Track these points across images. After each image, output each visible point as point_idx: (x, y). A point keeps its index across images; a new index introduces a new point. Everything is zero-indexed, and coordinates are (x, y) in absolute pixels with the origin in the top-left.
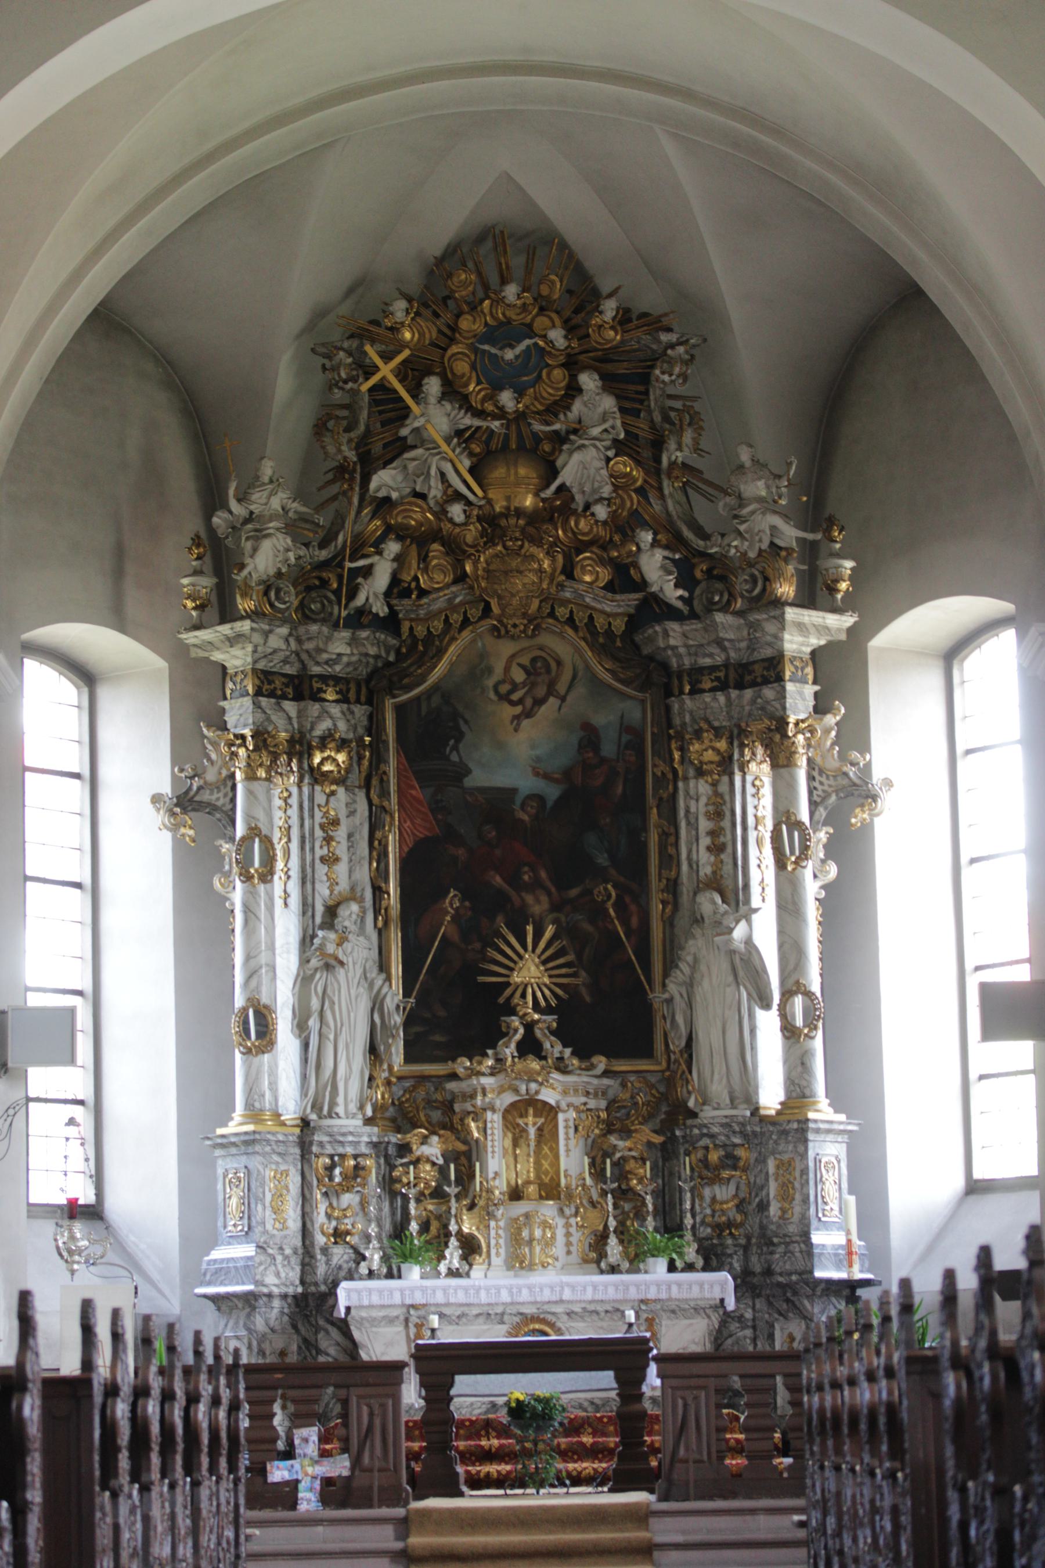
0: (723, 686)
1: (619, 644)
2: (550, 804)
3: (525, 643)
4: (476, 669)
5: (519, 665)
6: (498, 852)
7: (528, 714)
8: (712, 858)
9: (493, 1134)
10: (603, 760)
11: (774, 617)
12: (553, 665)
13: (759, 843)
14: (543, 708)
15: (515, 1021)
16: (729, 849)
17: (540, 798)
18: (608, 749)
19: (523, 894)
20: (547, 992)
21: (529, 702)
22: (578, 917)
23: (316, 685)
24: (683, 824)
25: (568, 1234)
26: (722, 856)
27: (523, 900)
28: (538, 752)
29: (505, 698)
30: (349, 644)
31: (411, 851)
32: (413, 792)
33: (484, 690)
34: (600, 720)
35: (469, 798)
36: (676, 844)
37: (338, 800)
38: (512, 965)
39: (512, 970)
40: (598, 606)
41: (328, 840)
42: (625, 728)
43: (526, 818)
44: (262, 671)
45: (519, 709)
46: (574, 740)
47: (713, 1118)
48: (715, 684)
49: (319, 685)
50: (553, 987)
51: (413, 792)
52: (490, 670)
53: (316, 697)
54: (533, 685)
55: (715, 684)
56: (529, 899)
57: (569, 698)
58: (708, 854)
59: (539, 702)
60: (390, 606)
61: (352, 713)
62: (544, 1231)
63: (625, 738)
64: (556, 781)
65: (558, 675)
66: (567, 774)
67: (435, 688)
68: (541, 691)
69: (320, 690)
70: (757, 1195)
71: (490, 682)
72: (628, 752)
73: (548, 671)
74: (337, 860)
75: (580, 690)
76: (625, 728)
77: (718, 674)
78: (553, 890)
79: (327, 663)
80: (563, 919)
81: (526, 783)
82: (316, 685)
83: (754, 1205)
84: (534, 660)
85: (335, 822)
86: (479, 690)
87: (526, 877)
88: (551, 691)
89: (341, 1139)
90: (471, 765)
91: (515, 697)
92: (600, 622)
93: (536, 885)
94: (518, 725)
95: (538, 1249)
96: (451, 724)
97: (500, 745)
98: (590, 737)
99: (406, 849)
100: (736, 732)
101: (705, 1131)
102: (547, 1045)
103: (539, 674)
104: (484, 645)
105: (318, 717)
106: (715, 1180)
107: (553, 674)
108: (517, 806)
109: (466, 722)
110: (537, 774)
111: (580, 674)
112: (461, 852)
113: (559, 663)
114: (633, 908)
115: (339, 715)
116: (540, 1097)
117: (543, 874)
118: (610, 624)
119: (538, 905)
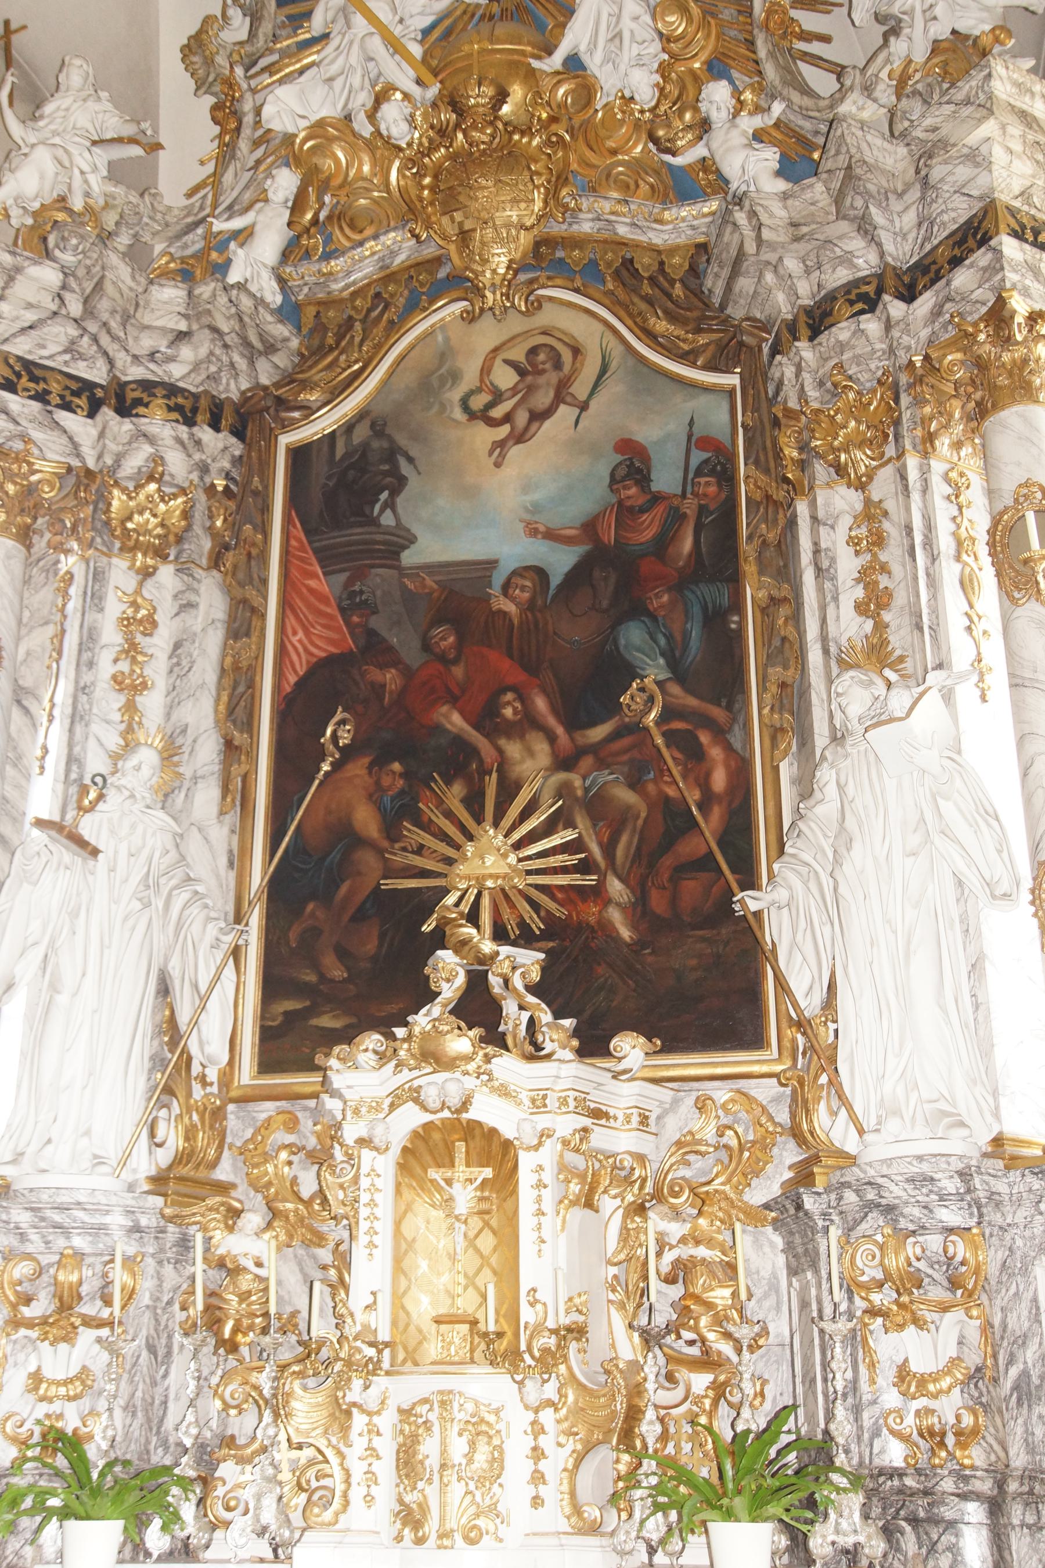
0: (871, 304)
1: (678, 290)
2: (555, 581)
3: (516, 324)
4: (434, 376)
5: (506, 362)
6: (458, 671)
7: (520, 437)
8: (869, 625)
9: (372, 1203)
10: (657, 498)
11: (967, 102)
12: (567, 356)
13: (967, 585)
14: (547, 424)
15: (446, 957)
16: (900, 598)
17: (540, 574)
18: (666, 478)
19: (502, 742)
20: (524, 907)
21: (522, 418)
22: (605, 777)
23: (131, 395)
24: (808, 577)
25: (538, 1453)
26: (887, 616)
27: (500, 751)
28: (536, 496)
29: (483, 416)
30: (186, 316)
31: (302, 683)
32: (312, 583)
33: (443, 407)
34: (647, 433)
35: (411, 586)
36: (797, 618)
37: (159, 587)
38: (451, 852)
39: (450, 861)
40: (643, 238)
41: (131, 650)
42: (697, 440)
43: (511, 608)
44: (19, 358)
45: (505, 430)
46: (604, 471)
47: (888, 1162)
48: (860, 306)
49: (137, 394)
50: (535, 894)
51: (312, 583)
52: (455, 376)
53: (124, 410)
54: (531, 389)
55: (860, 306)
56: (513, 749)
57: (593, 404)
58: (860, 619)
59: (539, 416)
60: (282, 281)
61: (198, 443)
62: (472, 1444)
63: (698, 457)
64: (568, 541)
65: (574, 371)
66: (590, 528)
67: (362, 415)
68: (543, 399)
69: (138, 402)
70: (1011, 1361)
71: (455, 395)
72: (703, 480)
73: (558, 365)
74: (144, 686)
75: (614, 388)
76: (697, 440)
77: (865, 289)
78: (560, 730)
79: (152, 356)
80: (578, 783)
81: (510, 548)
82: (131, 395)
83: (1008, 1384)
84: (533, 351)
85: (150, 624)
86: (436, 408)
87: (508, 712)
88: (560, 396)
89: (57, 1217)
90: (416, 529)
91: (497, 413)
92: (645, 263)
93: (530, 722)
94: (502, 456)
95: (457, 1490)
96: (387, 467)
97: (470, 492)
98: (633, 464)
99: (293, 679)
100: (904, 379)
101: (871, 1195)
102: (510, 1007)
103: (543, 372)
104: (447, 340)
105: (129, 443)
106: (906, 1316)
107: (567, 368)
108: (496, 590)
109: (411, 460)
110: (533, 532)
111: (614, 365)
112: (391, 678)
113: (576, 351)
114: (716, 753)
115: (170, 442)
116: (472, 1114)
117: (541, 704)
118: (662, 263)
119: (532, 763)
